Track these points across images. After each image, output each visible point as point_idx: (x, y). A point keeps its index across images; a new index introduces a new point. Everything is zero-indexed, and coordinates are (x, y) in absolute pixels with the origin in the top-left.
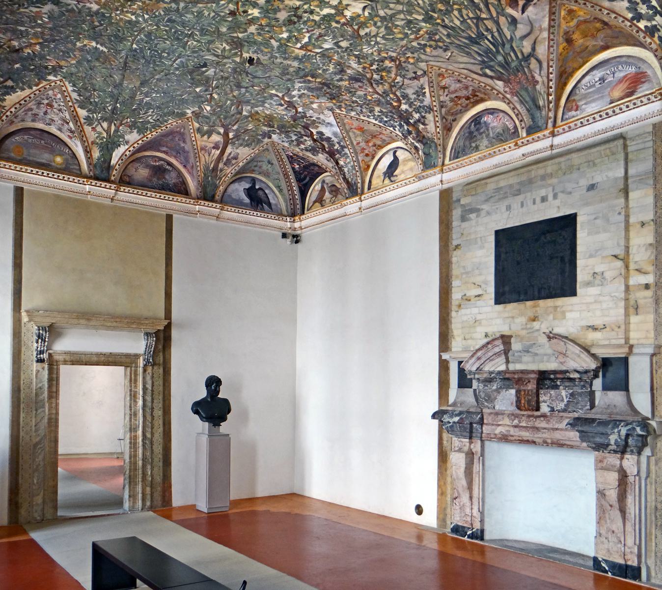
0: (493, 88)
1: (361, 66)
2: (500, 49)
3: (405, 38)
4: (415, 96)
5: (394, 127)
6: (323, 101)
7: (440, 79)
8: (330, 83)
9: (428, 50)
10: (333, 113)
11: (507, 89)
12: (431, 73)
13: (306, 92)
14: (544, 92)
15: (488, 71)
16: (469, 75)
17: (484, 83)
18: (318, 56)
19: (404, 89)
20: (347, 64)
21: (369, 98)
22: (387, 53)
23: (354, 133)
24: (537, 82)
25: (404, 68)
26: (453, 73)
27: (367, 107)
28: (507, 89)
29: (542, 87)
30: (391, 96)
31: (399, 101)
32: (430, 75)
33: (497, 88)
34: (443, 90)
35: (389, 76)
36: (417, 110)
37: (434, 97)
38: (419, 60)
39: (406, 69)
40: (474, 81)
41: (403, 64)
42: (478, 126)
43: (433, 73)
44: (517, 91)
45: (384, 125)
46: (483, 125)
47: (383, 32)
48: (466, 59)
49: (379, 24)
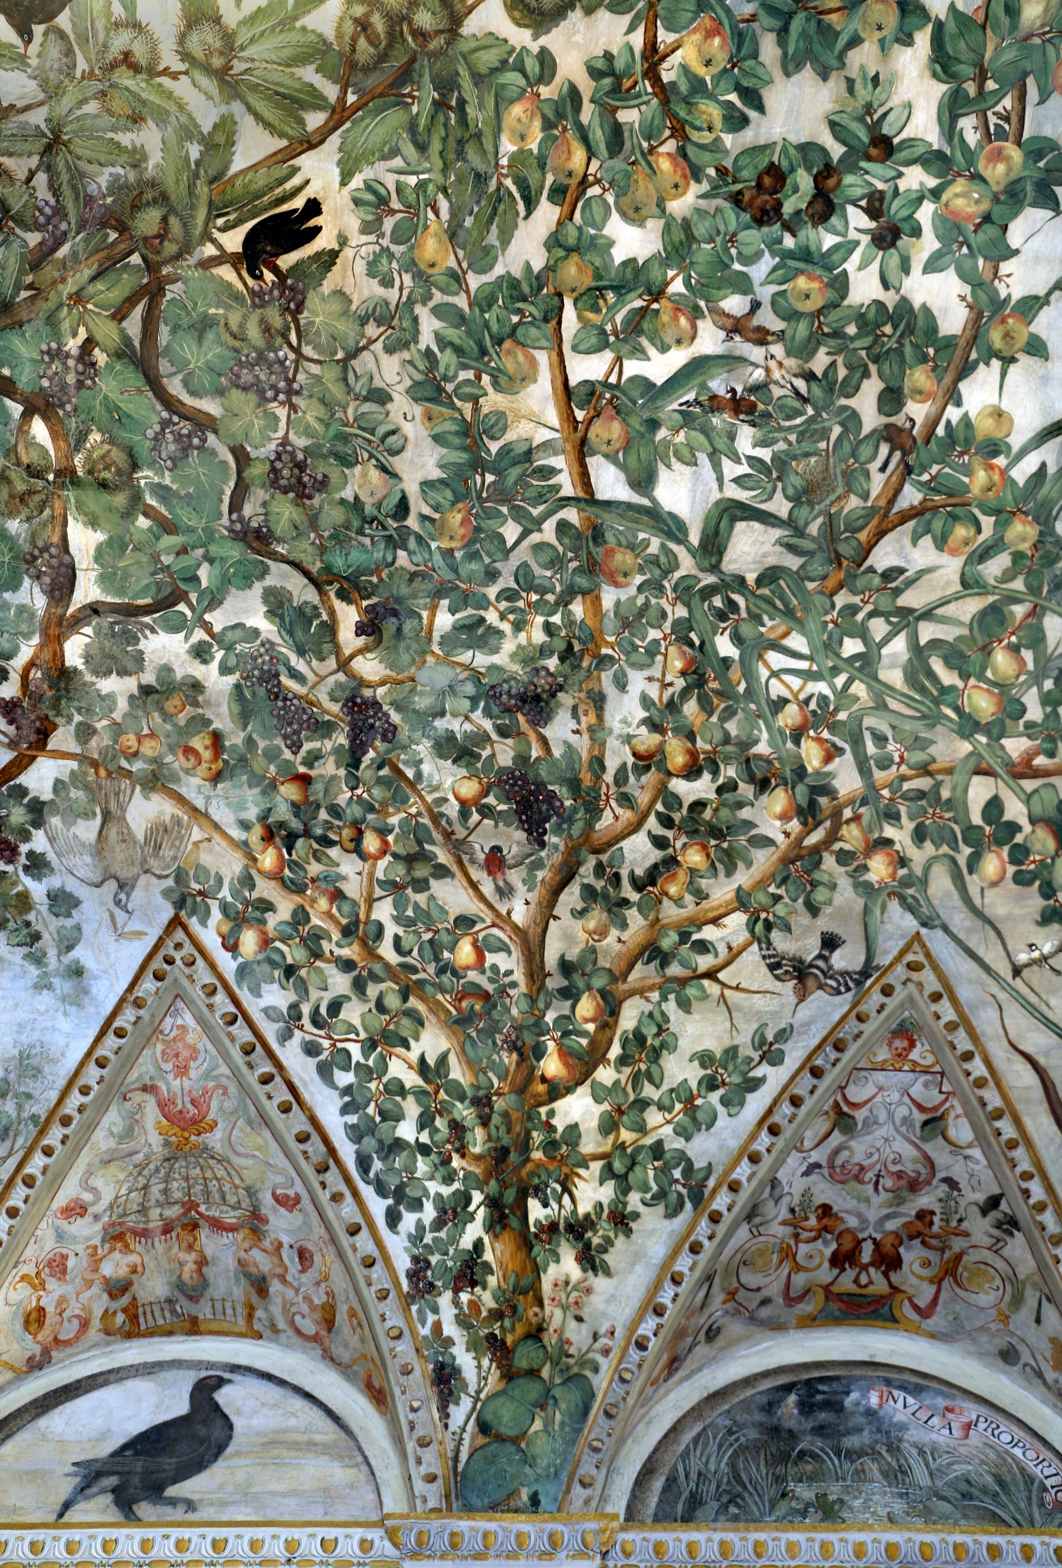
1: (647, 740)
3: (985, 729)
5: (402, 1197)
6: (221, 813)
8: (390, 733)
9: (992, 864)
10: (176, 922)
12: (887, 991)
13: (216, 680)
16: (1020, 1107)
18: (571, 515)
19: (685, 1005)
20: (606, 678)
22: (831, 753)
23: (132, 1127)
26: (968, 1056)
27: (393, 1001)
30: (586, 1007)
31: (583, 1065)
32: (876, 998)
35: (704, 883)
36: (619, 1170)
37: (774, 1131)
39: (820, 895)
40: (1019, 1153)
41: (829, 862)
42: (823, 1416)
43: (892, 1003)
45: (364, 1163)
46: (862, 1420)
47: (960, 623)
49: (995, 567)
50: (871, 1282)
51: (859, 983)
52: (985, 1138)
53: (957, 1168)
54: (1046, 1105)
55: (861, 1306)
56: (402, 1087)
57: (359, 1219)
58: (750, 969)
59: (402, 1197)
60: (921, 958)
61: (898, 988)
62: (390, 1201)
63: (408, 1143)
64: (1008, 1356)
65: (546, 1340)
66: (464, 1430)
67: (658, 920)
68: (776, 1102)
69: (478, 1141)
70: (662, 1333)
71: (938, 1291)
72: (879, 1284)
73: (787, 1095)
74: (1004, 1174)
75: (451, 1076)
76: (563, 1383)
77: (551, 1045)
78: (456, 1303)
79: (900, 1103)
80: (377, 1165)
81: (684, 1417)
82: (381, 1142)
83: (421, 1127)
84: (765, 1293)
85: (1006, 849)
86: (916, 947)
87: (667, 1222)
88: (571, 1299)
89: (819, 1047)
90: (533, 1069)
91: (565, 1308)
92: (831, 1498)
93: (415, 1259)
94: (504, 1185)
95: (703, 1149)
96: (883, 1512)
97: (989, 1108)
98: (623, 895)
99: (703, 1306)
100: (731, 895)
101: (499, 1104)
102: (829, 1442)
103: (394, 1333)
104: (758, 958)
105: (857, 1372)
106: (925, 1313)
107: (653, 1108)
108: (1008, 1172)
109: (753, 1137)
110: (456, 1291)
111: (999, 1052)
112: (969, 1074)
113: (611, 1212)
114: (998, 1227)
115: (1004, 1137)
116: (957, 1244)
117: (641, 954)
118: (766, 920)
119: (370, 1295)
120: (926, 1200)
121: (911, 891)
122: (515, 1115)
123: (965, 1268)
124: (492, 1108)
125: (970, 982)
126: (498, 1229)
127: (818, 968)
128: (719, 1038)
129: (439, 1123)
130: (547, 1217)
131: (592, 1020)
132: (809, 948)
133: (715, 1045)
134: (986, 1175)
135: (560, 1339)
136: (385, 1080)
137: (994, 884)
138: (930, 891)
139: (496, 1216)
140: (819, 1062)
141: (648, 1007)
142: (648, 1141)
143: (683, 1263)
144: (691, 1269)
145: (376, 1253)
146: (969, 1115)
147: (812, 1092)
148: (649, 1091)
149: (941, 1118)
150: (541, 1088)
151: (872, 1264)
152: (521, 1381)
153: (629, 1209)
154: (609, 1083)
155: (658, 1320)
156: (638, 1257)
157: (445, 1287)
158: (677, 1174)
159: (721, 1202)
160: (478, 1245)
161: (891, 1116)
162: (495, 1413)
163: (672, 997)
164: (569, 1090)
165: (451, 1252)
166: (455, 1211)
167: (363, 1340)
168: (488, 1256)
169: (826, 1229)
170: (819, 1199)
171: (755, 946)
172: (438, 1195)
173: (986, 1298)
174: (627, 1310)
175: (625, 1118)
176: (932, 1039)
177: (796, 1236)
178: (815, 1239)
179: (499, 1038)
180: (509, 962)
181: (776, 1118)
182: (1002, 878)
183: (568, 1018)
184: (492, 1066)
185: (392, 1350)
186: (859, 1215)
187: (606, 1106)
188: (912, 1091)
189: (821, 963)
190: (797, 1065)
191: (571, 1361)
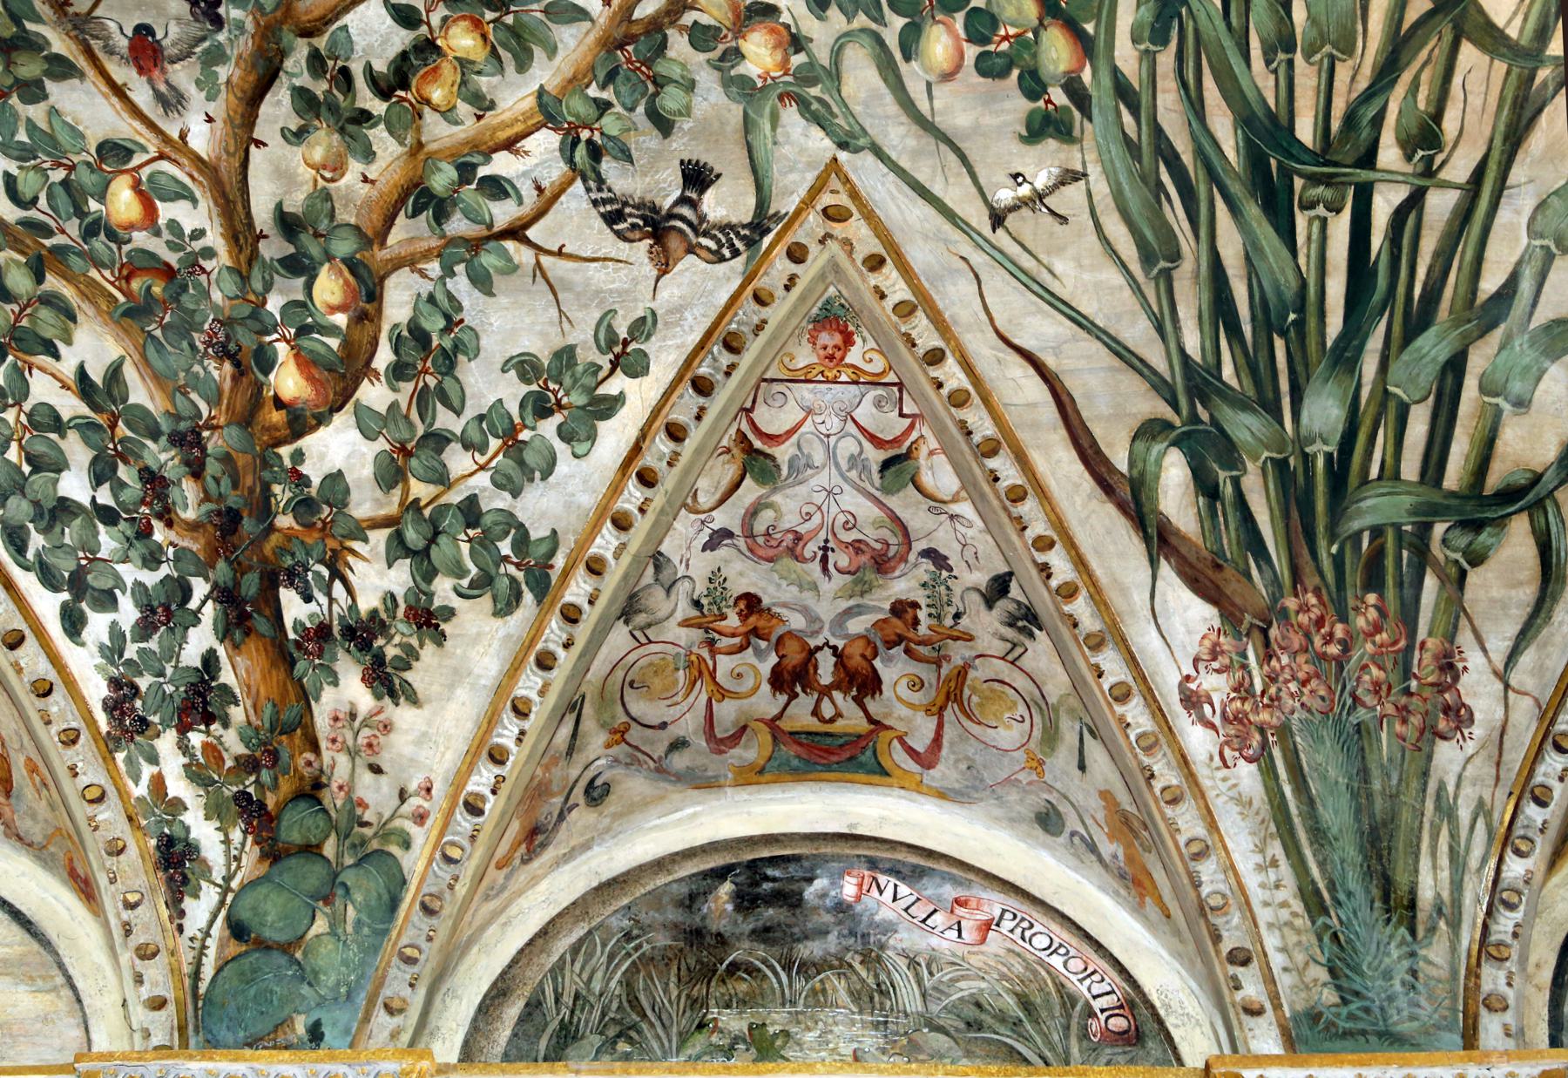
0: (1113, 634)
2: (1375, 343)
4: (511, 392)
7: (804, 356)
11: (1215, 685)
12: (797, 254)
14: (1481, 809)
15: (1173, 478)
16: (1023, 436)
17: (1080, 562)
19: (482, 282)
21: (122, 202)
24: (1460, 716)
25: (659, 82)
26: (935, 357)
28: (1215, 685)
29: (1482, 768)
32: (781, 266)
33: (1145, 639)
34: (730, 472)
37: (647, 479)
38: (808, 88)
39: (671, 100)
40: (1029, 508)
41: (678, 45)
44: (1284, 731)
48: (1096, 281)
50: (839, 715)
51: (751, 243)
52: (975, 485)
53: (940, 534)
54: (1063, 432)
55: (829, 752)
56: (58, 418)
57: (19, 624)
58: (575, 222)
59: (84, 590)
60: (843, 199)
61: (814, 248)
62: (66, 596)
63: (79, 506)
64: (1048, 821)
65: (327, 802)
66: (208, 934)
67: (420, 145)
68: (644, 434)
69: (189, 500)
70: (505, 789)
71: (940, 726)
72: (853, 721)
73: (659, 423)
74: (1009, 541)
75: (132, 400)
76: (357, 865)
77: (282, 349)
78: (184, 748)
79: (842, 434)
80: (37, 541)
81: (560, 915)
82: (36, 504)
83: (98, 480)
84: (675, 731)
85: (960, 17)
86: (834, 182)
87: (499, 622)
88: (361, 740)
89: (701, 346)
90: (259, 387)
91: (353, 754)
92: (771, 1030)
93: (115, 683)
94: (239, 568)
95: (540, 508)
96: (847, 1050)
97: (977, 438)
98: (360, 104)
99: (571, 750)
100: (530, 102)
101: (214, 443)
102: (776, 950)
103: (93, 793)
104: (586, 205)
105: (827, 849)
106: (927, 759)
107: (456, 447)
108: (1014, 537)
109: (616, 489)
110: (183, 729)
111: (982, 348)
112: (940, 385)
113: (409, 608)
114: (1011, 625)
115: (1003, 484)
116: (958, 653)
117: (401, 202)
118: (589, 142)
119: (50, 737)
120: (905, 584)
121: (815, 91)
122: (241, 460)
123: (974, 690)
124: (203, 449)
125: (926, 237)
126: (238, 635)
127: (683, 219)
128: (544, 335)
129: (123, 472)
130: (311, 616)
131: (341, 308)
132: (667, 188)
133: (541, 348)
134: (985, 544)
135: (349, 799)
136: (27, 407)
137: (948, 77)
138: (845, 92)
139: (233, 615)
140: (704, 370)
141: (426, 287)
142: (455, 497)
143: (529, 684)
144: (542, 693)
145: (52, 676)
146: (947, 449)
147: (699, 418)
148: (445, 419)
149: (908, 456)
150: (277, 417)
151: (836, 685)
152: (293, 862)
153: (437, 603)
154: (382, 408)
155: (497, 770)
156: (458, 675)
157: (166, 724)
158: (505, 547)
159: (578, 590)
160: (210, 660)
161: (831, 454)
162: (254, 909)
163: (460, 268)
164: (321, 420)
165: (169, 671)
166: (167, 609)
167: (52, 807)
168: (227, 676)
169: (755, 632)
170: (738, 587)
171: (579, 183)
172: (138, 584)
173: (1008, 735)
174: (449, 756)
175: (414, 462)
176: (877, 331)
177: (711, 643)
178: (741, 649)
179: (199, 339)
180: (195, 216)
181: (647, 460)
182: (958, 67)
183: (302, 305)
184: (195, 383)
185: (91, 819)
186: (805, 611)
187: (382, 445)
188: (857, 414)
189: (686, 211)
190: (671, 375)
191: (368, 832)
